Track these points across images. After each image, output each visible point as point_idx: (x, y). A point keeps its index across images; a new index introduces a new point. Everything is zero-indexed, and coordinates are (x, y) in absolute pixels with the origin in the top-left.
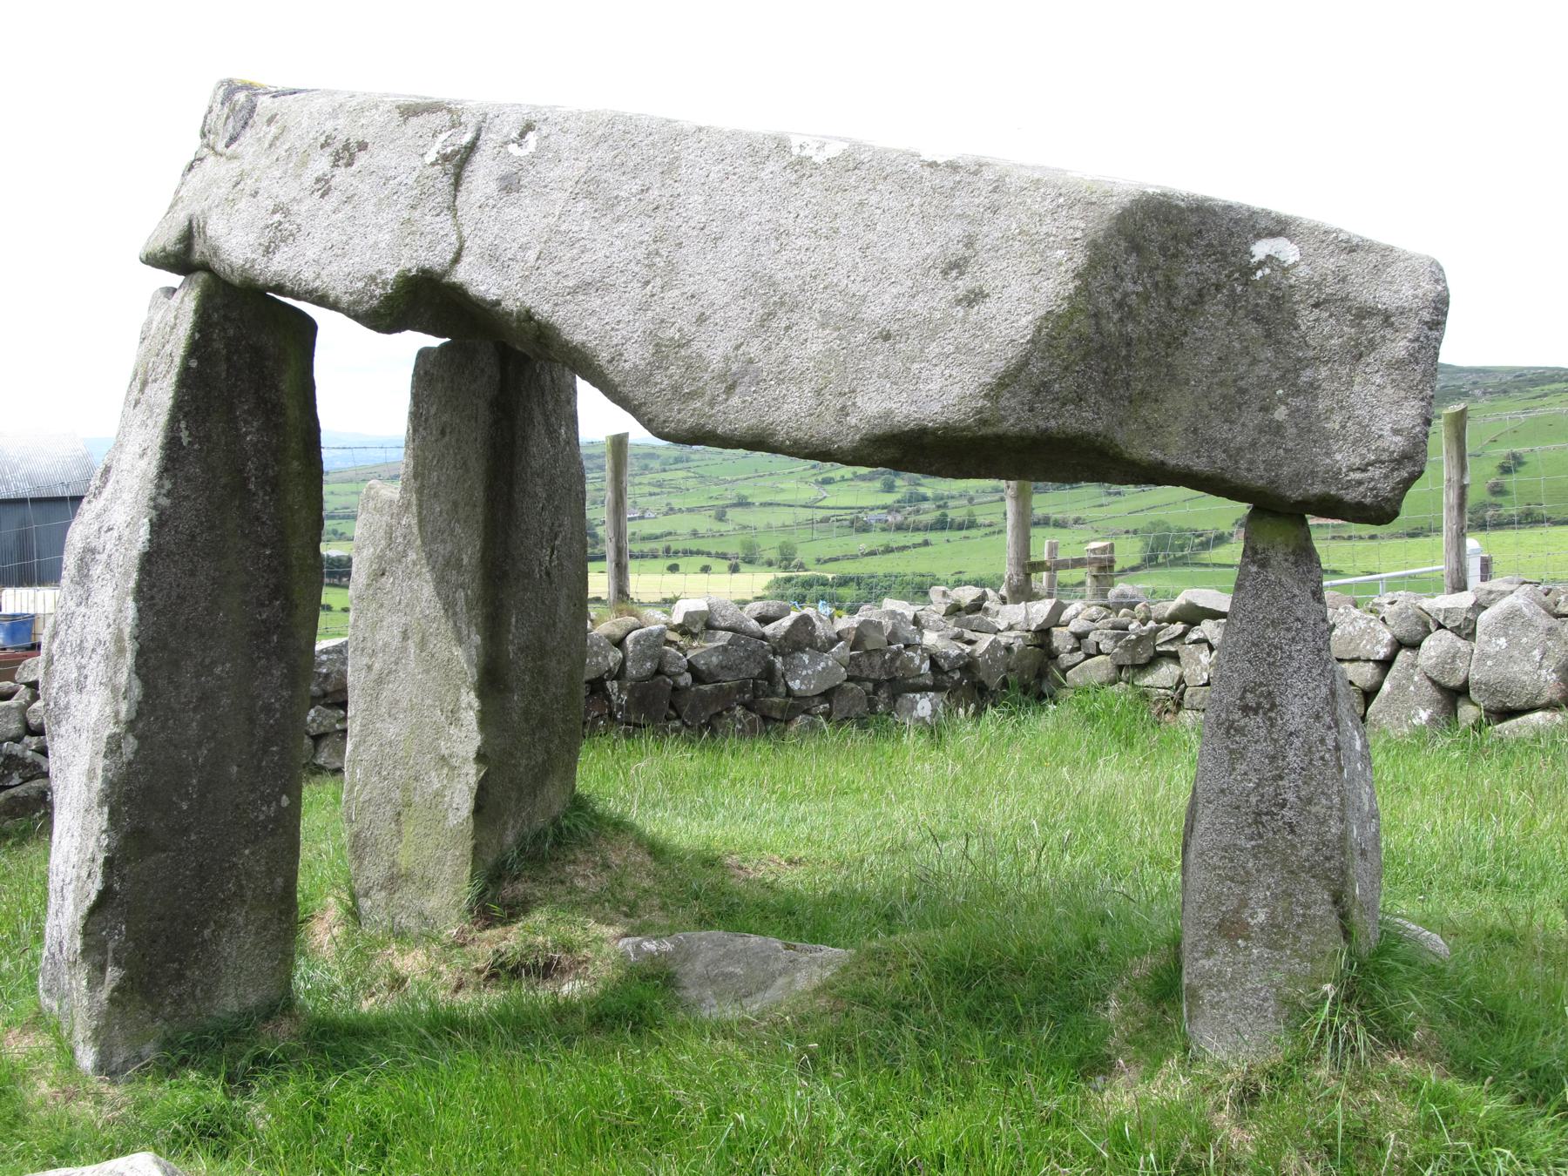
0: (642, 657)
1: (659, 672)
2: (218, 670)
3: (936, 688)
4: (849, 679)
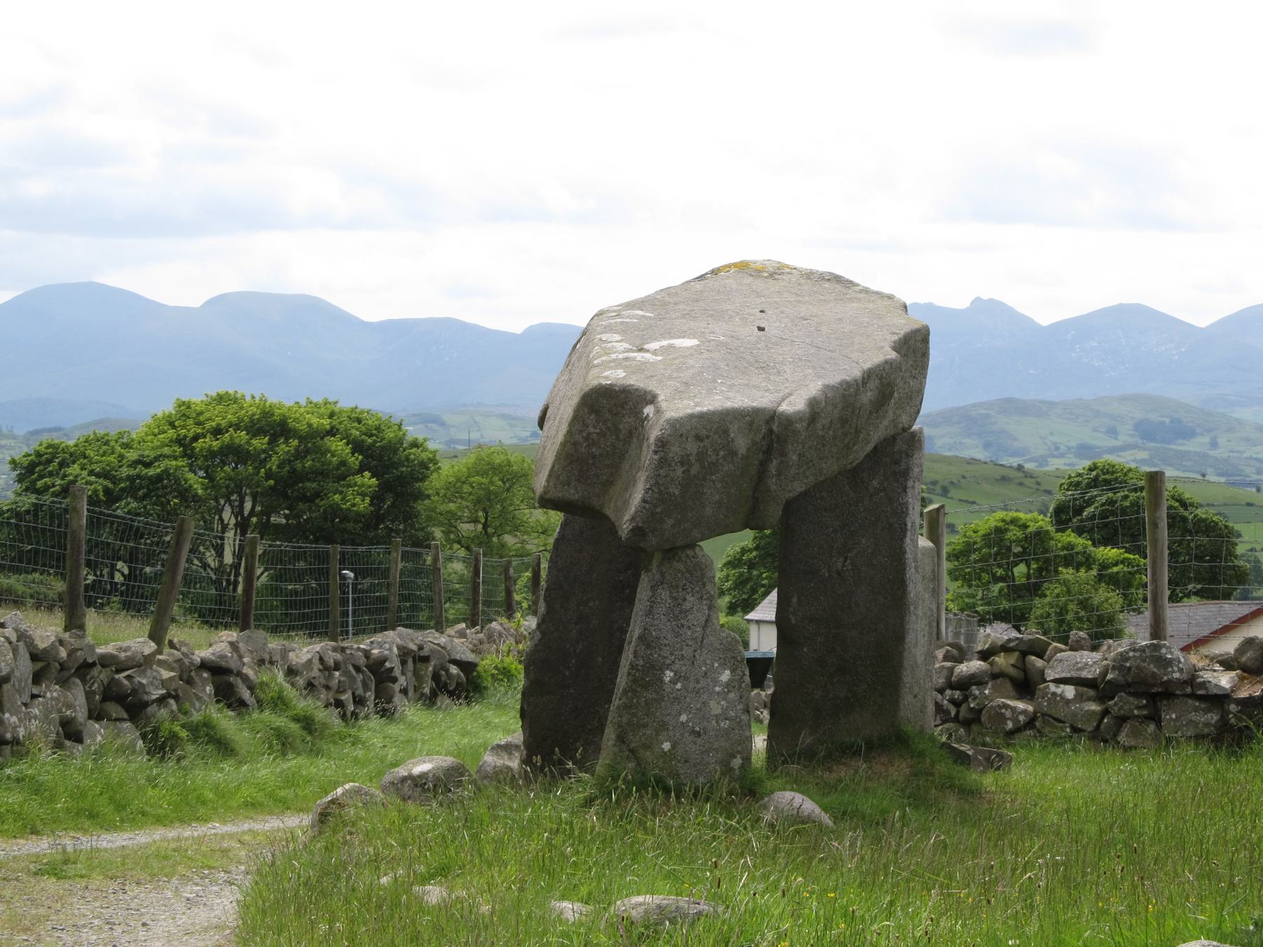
2: (591, 604)
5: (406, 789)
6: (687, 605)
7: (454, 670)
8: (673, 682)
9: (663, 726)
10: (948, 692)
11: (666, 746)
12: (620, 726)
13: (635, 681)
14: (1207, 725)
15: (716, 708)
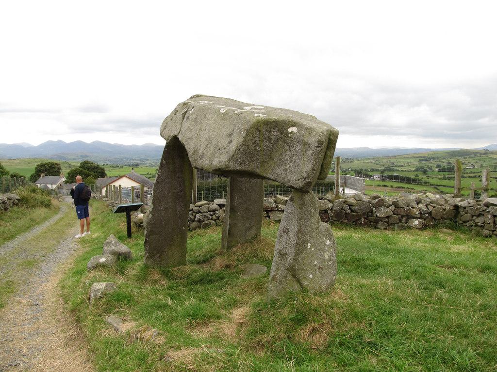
1: (342, 209)
3: (420, 218)
4: (394, 214)
7: (16, 201)
8: (311, 248)
11: (311, 276)
15: (327, 257)
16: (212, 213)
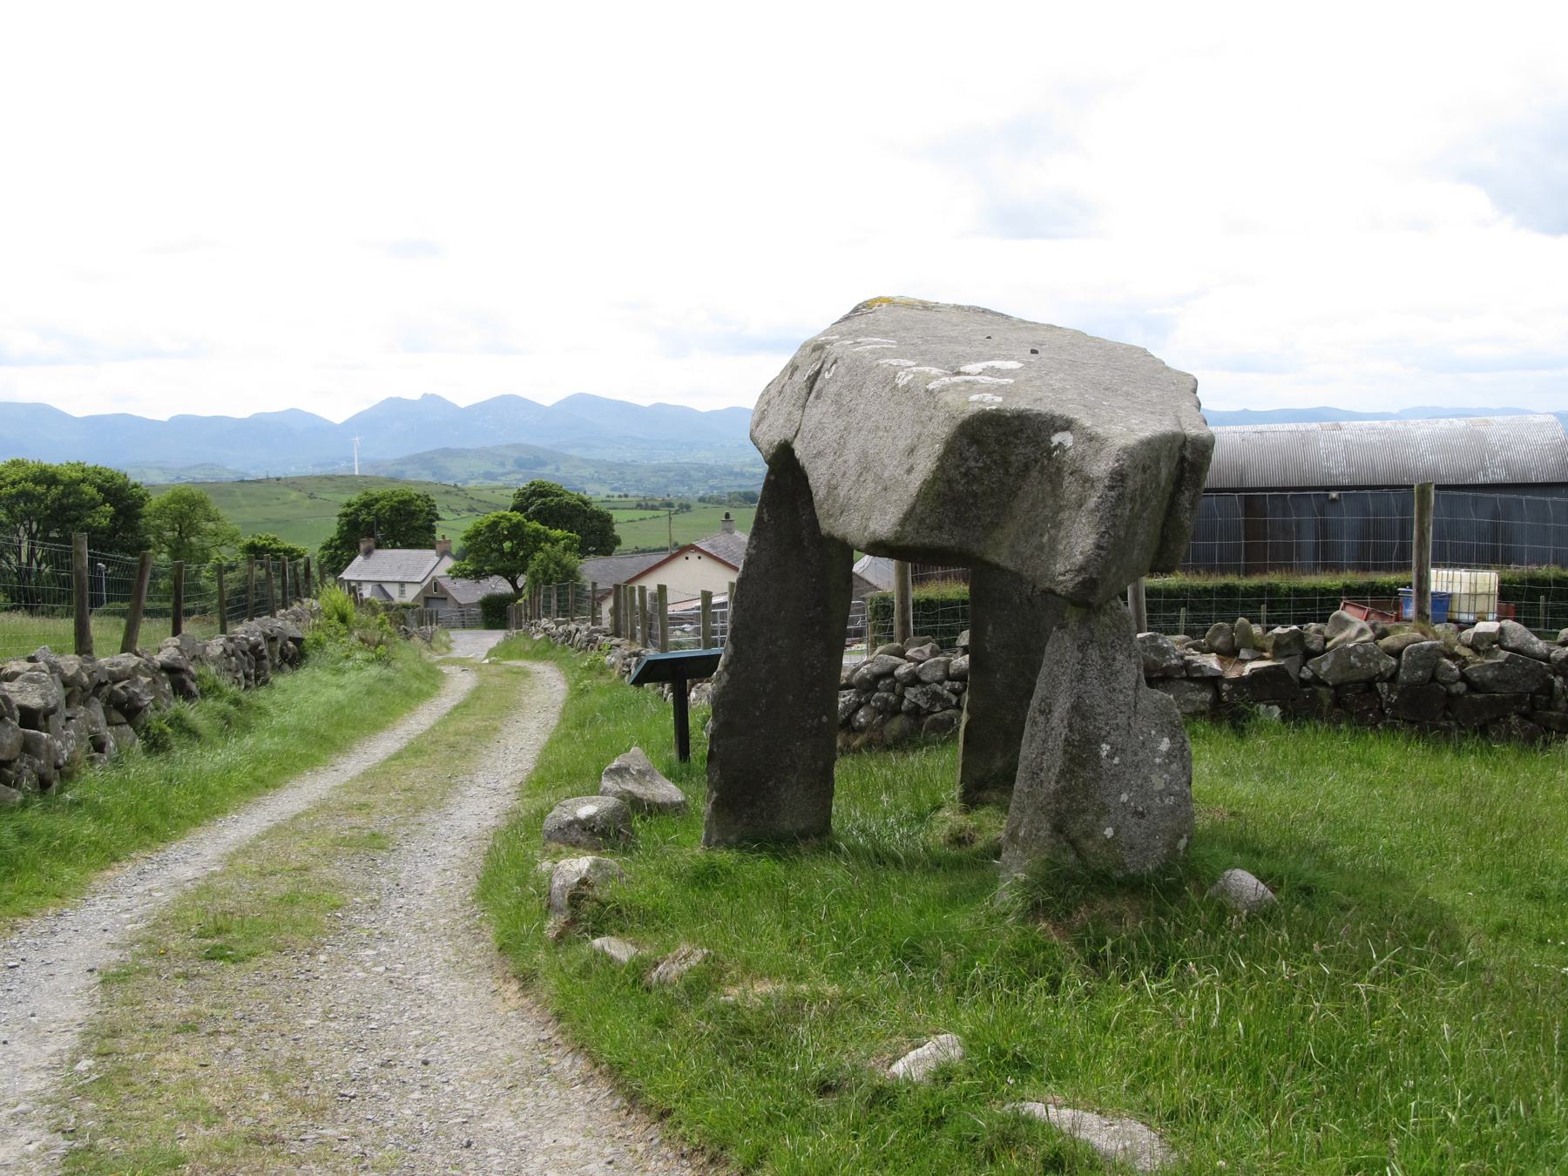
0: (1414, 666)
1: (1434, 678)
5: (574, 834)
6: (1118, 665)
7: (291, 645)
8: (1110, 756)
9: (1104, 810)
10: (948, 684)
11: (1109, 832)
12: (1058, 814)
13: (1071, 760)
14: (1203, 702)
15: (1158, 784)
16: (957, 685)
